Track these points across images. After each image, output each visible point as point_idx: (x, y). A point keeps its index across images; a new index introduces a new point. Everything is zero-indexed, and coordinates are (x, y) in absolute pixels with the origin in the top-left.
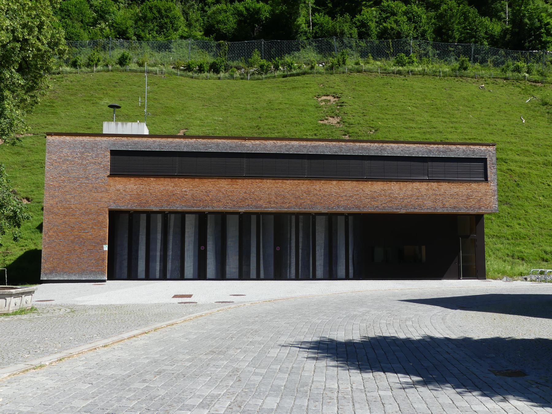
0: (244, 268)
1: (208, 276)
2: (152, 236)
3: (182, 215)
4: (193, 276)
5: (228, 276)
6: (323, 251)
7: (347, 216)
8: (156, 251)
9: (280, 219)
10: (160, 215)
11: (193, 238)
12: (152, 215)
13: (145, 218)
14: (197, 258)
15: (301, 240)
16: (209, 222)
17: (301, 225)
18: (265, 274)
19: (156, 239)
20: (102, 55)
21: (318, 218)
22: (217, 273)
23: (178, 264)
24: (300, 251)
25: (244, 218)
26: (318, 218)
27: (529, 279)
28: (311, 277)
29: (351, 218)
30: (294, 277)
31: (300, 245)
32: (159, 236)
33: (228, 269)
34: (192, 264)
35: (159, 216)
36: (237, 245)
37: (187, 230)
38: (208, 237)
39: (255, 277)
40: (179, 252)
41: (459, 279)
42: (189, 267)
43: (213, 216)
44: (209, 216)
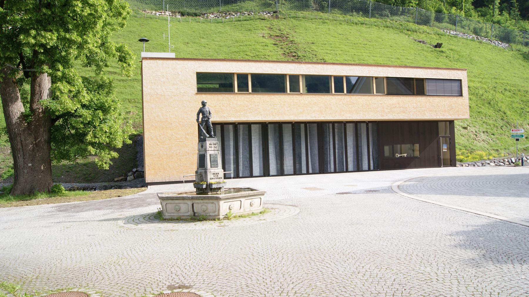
0: (297, 166)
1: (271, 174)
2: (226, 143)
3: (248, 125)
4: (260, 173)
5: (286, 173)
6: (352, 150)
7: (368, 123)
8: (230, 155)
9: (322, 127)
10: (220, 126)
11: (258, 144)
12: (225, 126)
13: (220, 129)
14: (262, 159)
15: (336, 142)
16: (269, 130)
17: (336, 130)
18: (312, 169)
19: (230, 145)
20: (118, 6)
21: (348, 125)
22: (277, 171)
23: (247, 164)
24: (337, 151)
25: (295, 125)
26: (348, 125)
27: (464, 165)
28: (345, 170)
29: (370, 125)
30: (333, 171)
31: (337, 146)
32: (232, 143)
33: (285, 168)
34: (258, 164)
35: (231, 127)
36: (291, 148)
37: (253, 137)
38: (269, 142)
39: (305, 172)
40: (248, 156)
41: (440, 167)
42: (257, 168)
43: (272, 125)
44: (269, 125)
